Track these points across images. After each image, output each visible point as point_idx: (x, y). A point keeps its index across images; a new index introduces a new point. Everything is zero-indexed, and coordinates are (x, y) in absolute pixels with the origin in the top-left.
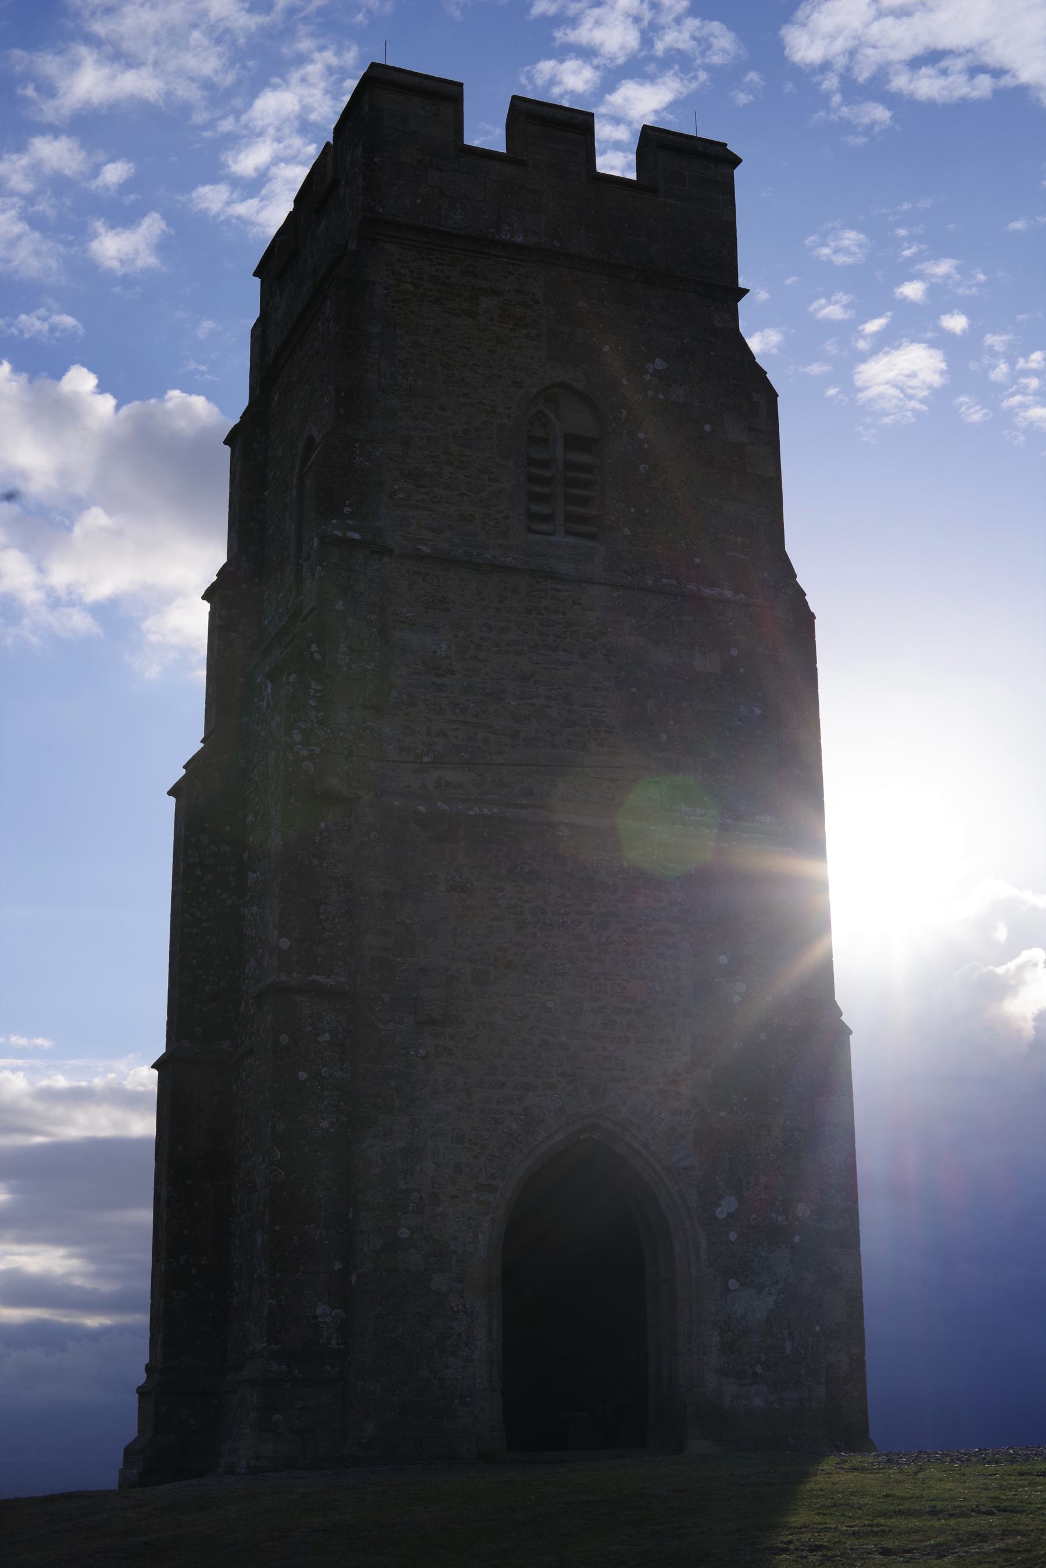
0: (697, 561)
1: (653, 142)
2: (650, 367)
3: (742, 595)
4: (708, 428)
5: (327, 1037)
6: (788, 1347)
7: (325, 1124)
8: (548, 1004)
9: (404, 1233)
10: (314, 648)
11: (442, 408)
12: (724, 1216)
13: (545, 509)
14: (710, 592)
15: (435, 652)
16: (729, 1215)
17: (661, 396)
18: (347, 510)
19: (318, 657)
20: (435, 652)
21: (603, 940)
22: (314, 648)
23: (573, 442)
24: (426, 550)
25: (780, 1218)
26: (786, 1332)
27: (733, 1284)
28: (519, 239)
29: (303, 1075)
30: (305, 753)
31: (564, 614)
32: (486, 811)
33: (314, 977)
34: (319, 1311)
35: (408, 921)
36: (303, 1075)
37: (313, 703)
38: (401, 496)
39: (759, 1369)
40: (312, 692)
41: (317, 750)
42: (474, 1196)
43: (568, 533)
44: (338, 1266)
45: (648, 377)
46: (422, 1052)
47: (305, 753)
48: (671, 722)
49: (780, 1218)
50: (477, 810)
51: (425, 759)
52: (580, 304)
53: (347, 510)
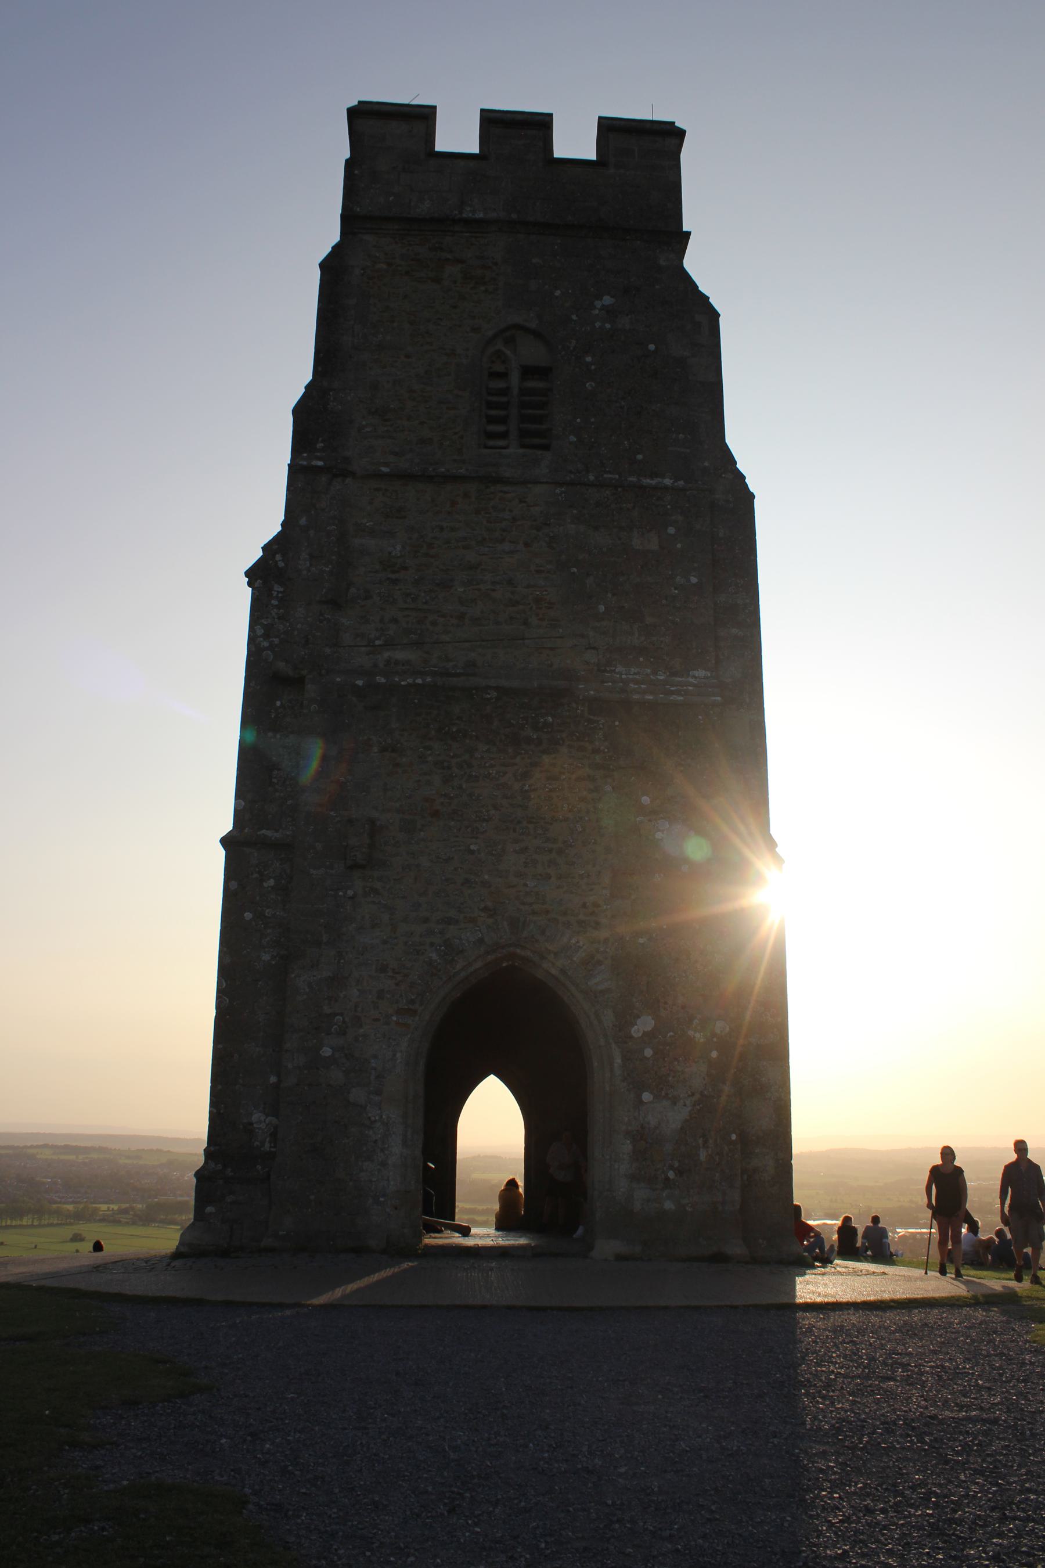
0: (640, 457)
1: (610, 129)
2: (598, 304)
3: (681, 483)
4: (652, 347)
5: (272, 882)
6: (703, 1155)
7: (266, 957)
8: (472, 847)
9: (326, 1052)
10: (278, 557)
11: (408, 356)
12: (640, 1035)
13: (500, 428)
14: (648, 481)
15: (390, 553)
16: (645, 1034)
17: (608, 326)
18: (320, 445)
19: (281, 564)
20: (390, 553)
21: (527, 788)
22: (278, 557)
23: (528, 372)
24: (385, 470)
25: (697, 1035)
26: (701, 1141)
27: (647, 1096)
28: (480, 215)
29: (248, 916)
30: (266, 644)
31: (511, 511)
32: (419, 681)
33: (264, 831)
34: (255, 1117)
35: (342, 779)
36: (248, 916)
37: (275, 602)
38: (368, 429)
39: (671, 1175)
40: (275, 594)
41: (276, 641)
42: (394, 1018)
43: (523, 446)
44: (273, 1079)
45: (597, 312)
46: (350, 893)
47: (266, 644)
48: (609, 595)
49: (697, 1035)
50: (410, 681)
51: (377, 643)
52: (534, 261)
53: (320, 445)
